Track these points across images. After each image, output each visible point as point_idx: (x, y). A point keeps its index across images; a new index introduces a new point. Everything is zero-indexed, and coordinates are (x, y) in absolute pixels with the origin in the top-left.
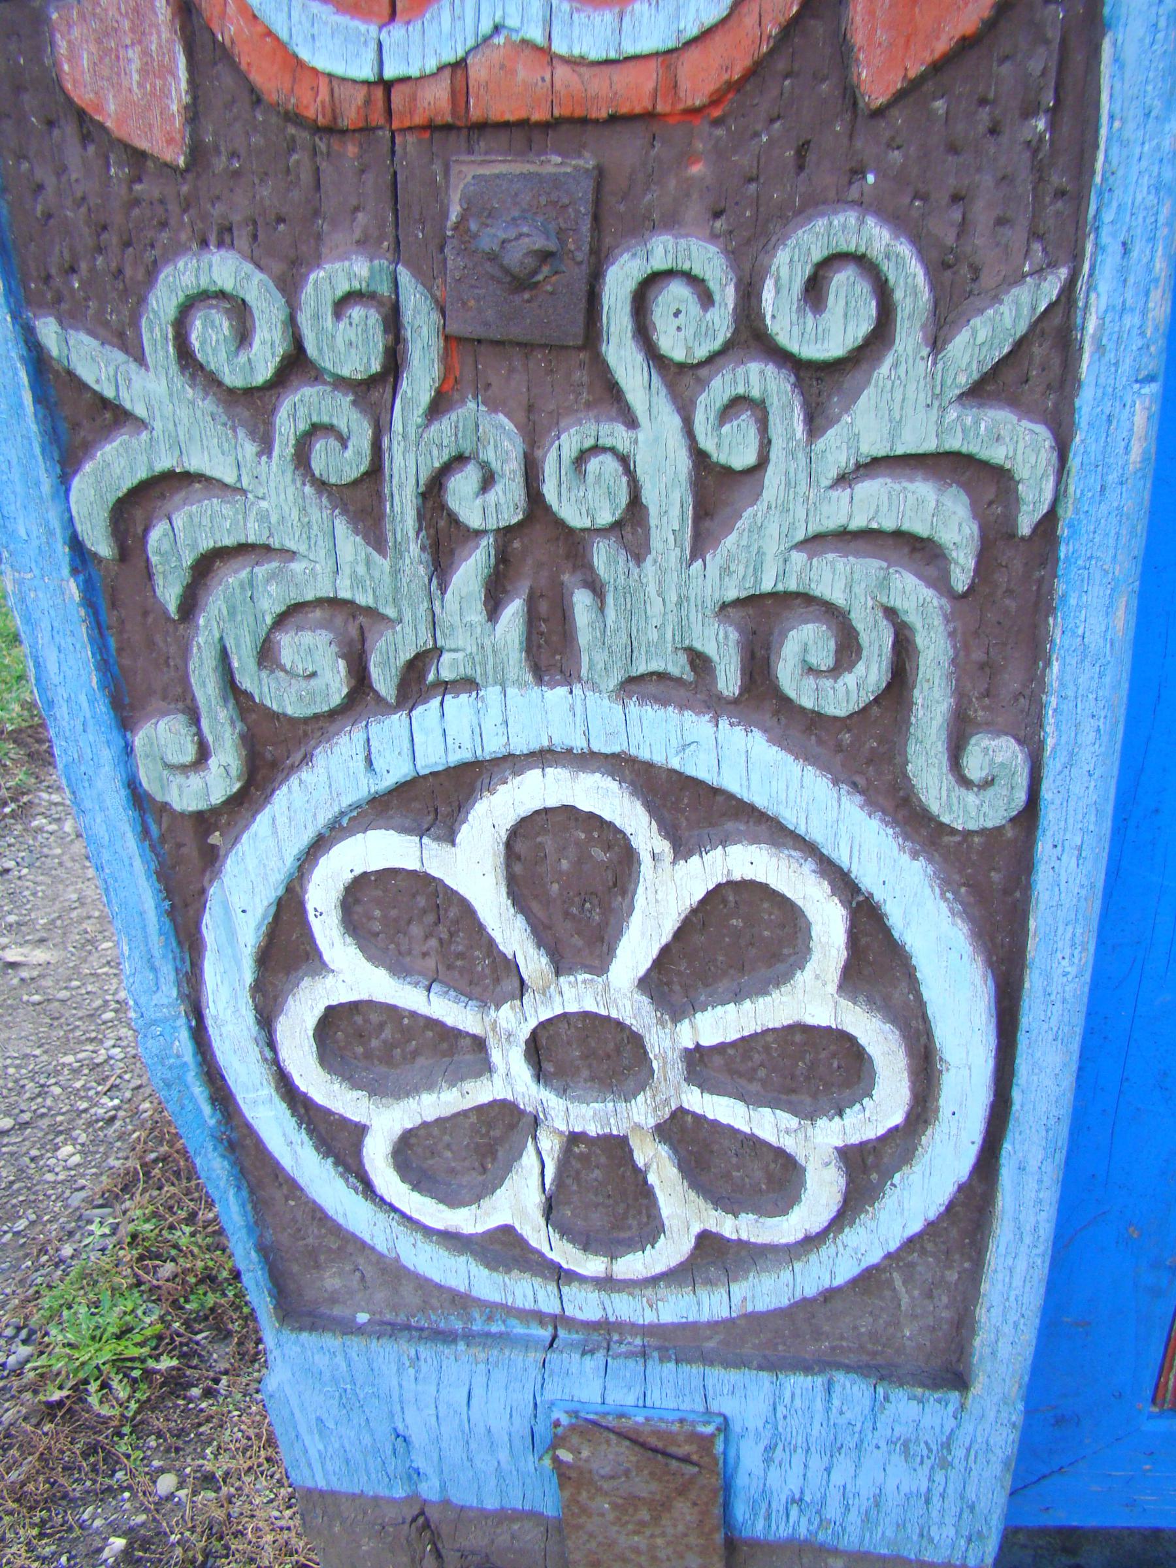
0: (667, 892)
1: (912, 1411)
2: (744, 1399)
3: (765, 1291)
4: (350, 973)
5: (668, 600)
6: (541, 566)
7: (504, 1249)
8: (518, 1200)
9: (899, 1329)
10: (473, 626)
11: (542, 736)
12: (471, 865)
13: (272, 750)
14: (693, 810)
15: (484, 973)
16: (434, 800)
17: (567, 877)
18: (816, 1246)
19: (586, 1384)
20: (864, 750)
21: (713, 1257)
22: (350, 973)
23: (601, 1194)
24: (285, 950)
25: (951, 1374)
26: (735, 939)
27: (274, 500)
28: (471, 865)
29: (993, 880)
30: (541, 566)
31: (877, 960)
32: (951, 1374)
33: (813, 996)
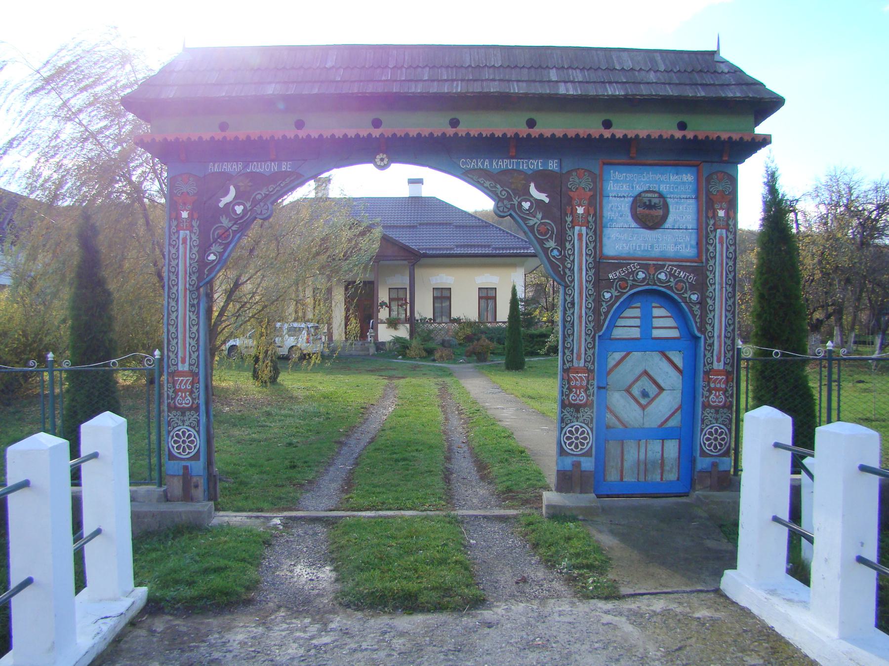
0: (581, 430)
1: (590, 459)
2: (582, 459)
3: (583, 451)
4: (568, 435)
5: (581, 419)
6: (577, 418)
7: (572, 450)
8: (573, 447)
9: (588, 454)
10: (575, 420)
11: (576, 424)
12: (573, 430)
13: (567, 424)
14: (582, 427)
15: (573, 434)
16: (572, 427)
17: (577, 430)
18: (586, 448)
19: (575, 459)
20: (587, 424)
21: (582, 449)
22: (568, 435)
23: (576, 447)
24: (565, 433)
25: (591, 456)
26: (583, 432)
27: (568, 415)
28: (573, 430)
29: (591, 429)
30: (577, 418)
31: (588, 434)
32: (591, 456)
33: (585, 435)
